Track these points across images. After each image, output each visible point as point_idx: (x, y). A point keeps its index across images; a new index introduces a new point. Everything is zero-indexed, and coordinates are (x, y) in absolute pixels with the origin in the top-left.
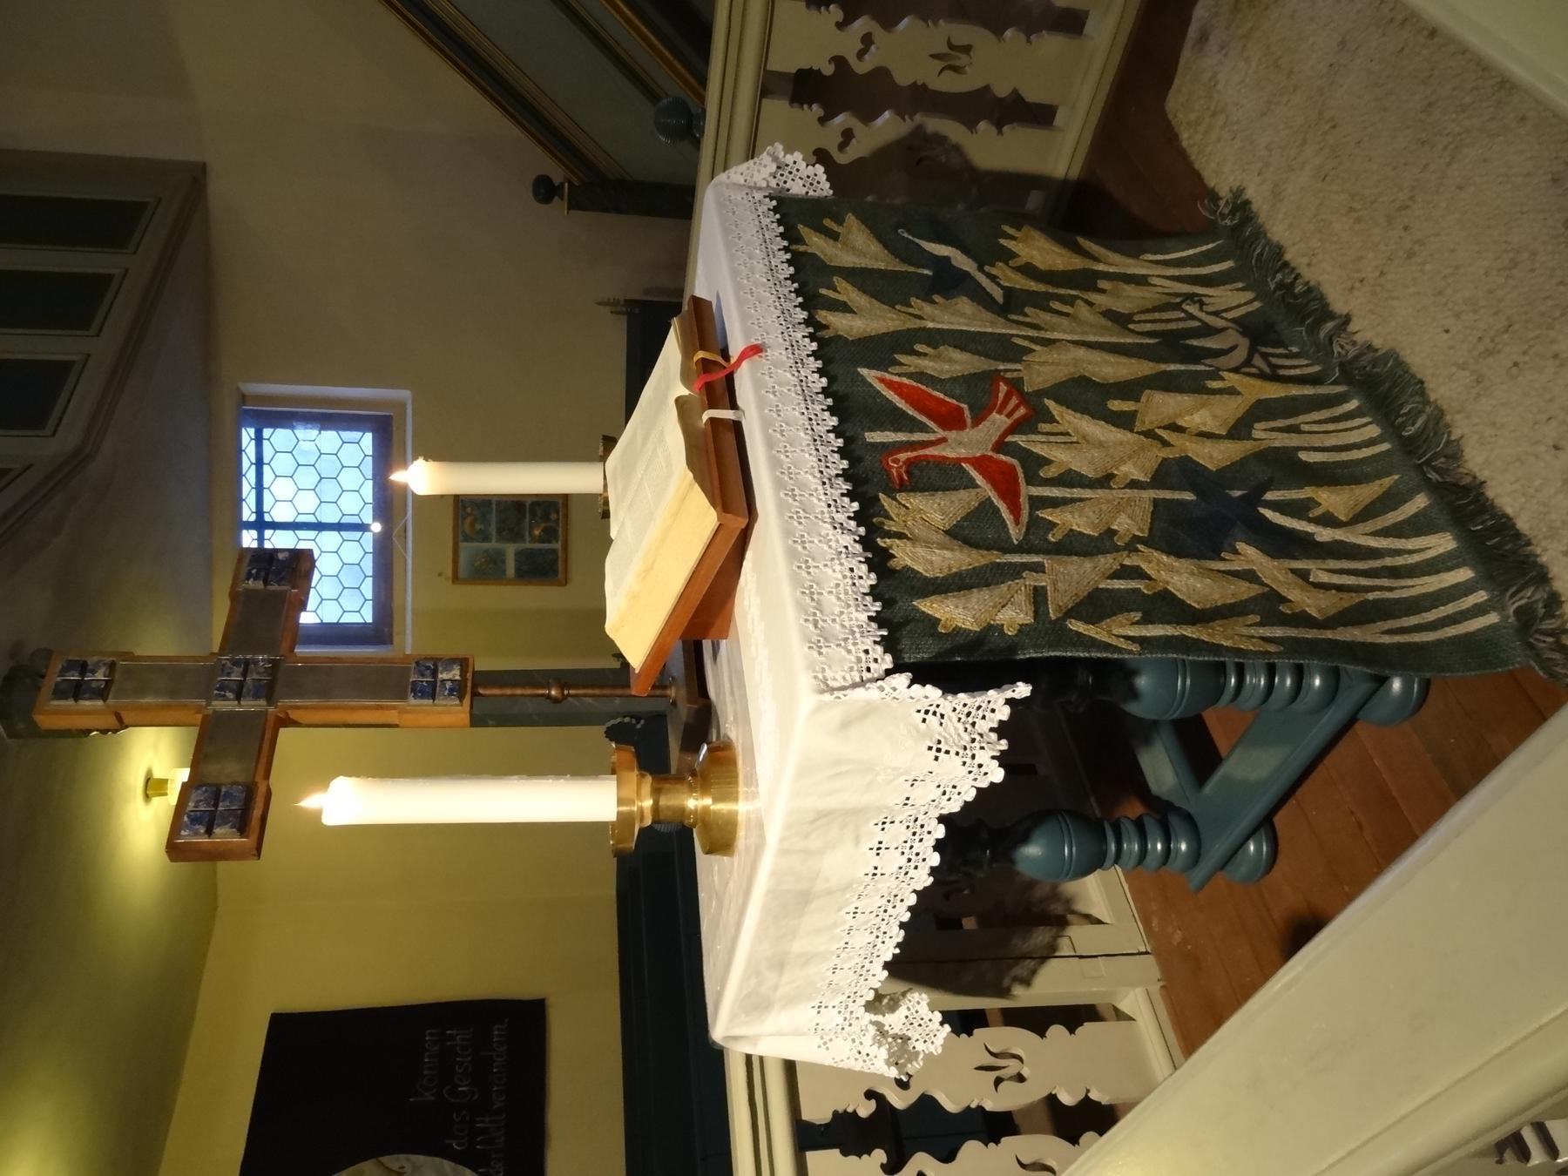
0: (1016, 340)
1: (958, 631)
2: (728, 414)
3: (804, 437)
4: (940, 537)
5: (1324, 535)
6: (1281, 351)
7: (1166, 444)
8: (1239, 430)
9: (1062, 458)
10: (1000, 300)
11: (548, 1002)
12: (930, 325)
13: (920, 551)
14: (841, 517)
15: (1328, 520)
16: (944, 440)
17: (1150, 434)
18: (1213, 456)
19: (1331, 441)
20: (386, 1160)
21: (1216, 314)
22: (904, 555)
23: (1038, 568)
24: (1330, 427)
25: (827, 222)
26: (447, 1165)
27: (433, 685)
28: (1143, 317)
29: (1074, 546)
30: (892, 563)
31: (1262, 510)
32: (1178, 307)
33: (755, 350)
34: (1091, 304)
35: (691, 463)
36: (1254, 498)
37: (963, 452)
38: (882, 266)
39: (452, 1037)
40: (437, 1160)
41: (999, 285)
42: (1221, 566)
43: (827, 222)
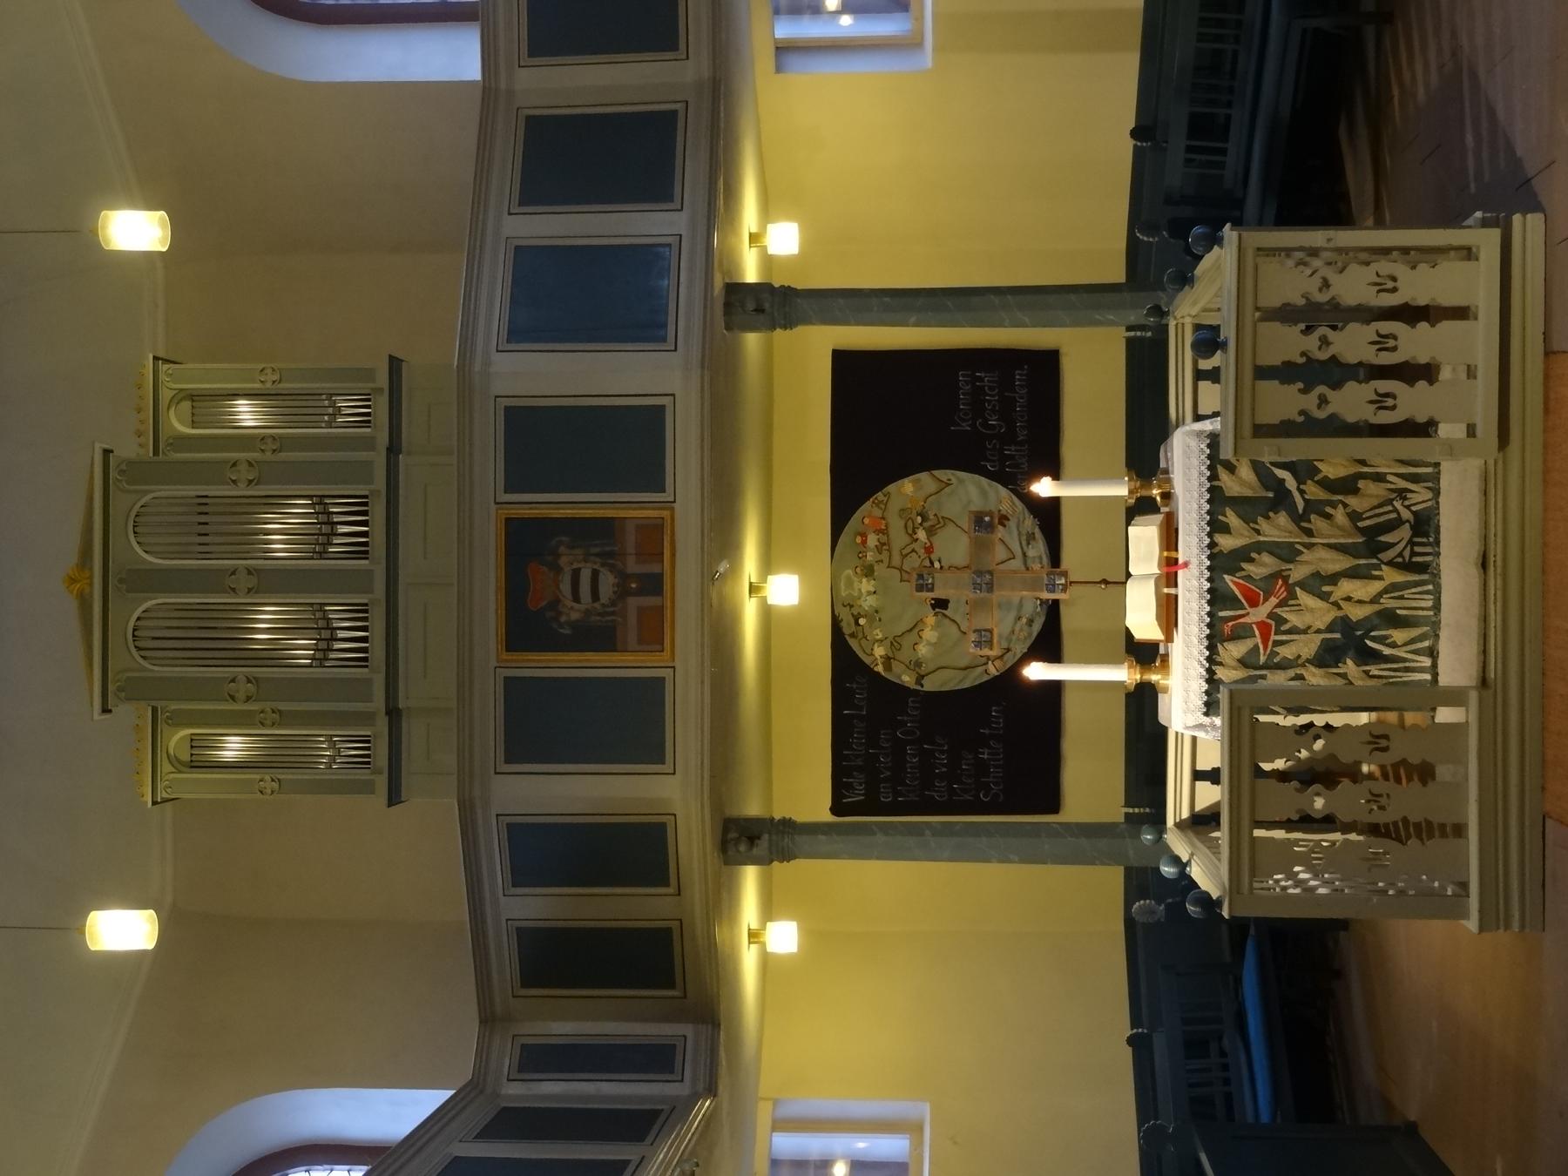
2: (1172, 591)
4: (1235, 664)
5: (1387, 651)
7: (1340, 608)
8: (1374, 600)
9: (1294, 619)
15: (1394, 645)
17: (1336, 605)
18: (1356, 613)
19: (1414, 604)
20: (936, 473)
21: (1408, 507)
22: (1221, 673)
23: (1263, 677)
26: (984, 481)
29: (1283, 666)
33: (1186, 565)
34: (1345, 505)
35: (1158, 618)
36: (1366, 635)
38: (1249, 493)
39: (981, 379)
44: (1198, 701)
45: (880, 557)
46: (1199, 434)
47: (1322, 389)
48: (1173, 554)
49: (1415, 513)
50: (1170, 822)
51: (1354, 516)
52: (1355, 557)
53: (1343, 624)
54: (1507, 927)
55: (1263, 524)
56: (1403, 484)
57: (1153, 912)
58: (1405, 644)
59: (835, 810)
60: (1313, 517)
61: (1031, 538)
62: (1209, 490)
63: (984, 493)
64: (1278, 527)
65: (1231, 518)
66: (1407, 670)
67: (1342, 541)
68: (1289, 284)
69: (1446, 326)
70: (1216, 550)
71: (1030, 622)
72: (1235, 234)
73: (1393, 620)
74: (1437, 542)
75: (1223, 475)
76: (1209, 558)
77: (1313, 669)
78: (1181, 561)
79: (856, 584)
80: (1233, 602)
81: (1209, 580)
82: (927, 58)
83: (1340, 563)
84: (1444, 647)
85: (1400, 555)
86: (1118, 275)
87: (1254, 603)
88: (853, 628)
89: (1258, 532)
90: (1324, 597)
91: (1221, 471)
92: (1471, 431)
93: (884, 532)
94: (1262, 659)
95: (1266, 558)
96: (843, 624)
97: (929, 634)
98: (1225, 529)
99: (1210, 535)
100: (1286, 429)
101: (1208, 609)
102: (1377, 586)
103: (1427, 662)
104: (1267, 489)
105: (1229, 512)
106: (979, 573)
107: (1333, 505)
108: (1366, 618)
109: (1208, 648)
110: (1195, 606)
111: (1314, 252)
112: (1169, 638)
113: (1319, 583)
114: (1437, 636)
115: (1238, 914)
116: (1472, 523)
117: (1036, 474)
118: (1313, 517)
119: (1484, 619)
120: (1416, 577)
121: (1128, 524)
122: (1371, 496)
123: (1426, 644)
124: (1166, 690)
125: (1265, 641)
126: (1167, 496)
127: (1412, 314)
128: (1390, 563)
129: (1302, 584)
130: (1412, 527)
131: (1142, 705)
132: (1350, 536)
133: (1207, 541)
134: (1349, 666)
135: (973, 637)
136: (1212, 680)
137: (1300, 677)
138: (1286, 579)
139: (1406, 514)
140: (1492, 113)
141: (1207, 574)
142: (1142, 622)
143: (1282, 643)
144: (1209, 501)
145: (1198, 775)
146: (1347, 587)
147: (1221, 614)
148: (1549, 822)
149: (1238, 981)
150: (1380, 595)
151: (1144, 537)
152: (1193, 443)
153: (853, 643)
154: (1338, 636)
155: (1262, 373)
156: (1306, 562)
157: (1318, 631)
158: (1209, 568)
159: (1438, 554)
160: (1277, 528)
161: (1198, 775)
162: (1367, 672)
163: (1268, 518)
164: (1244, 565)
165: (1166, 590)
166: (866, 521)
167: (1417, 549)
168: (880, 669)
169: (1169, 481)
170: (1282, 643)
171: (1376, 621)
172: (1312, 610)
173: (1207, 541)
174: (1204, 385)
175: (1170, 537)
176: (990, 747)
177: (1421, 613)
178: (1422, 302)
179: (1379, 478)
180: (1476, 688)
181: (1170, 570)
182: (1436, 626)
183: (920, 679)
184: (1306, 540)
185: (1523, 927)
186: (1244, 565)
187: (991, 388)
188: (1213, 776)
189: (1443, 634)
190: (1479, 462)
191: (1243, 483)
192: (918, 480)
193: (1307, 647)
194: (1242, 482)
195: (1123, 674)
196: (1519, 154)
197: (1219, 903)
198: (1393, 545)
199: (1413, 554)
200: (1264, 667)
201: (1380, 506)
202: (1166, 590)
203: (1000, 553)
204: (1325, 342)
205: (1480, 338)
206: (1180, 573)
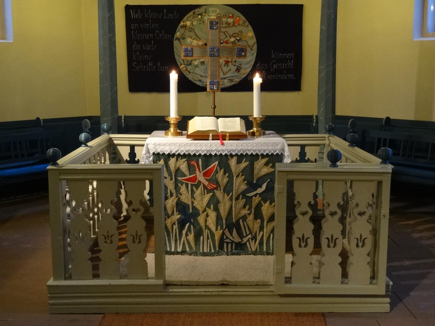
0: (231, 194)
2: (211, 138)
3: (198, 149)
4: (177, 166)
5: (184, 232)
6: (234, 248)
7: (203, 212)
8: (207, 227)
9: (198, 192)
10: (247, 195)
11: (300, 92)
12: (235, 178)
13: (174, 162)
14: (179, 151)
15: (187, 235)
16: (200, 172)
17: (205, 211)
18: (201, 219)
19: (205, 244)
21: (248, 241)
23: (171, 179)
24: (209, 245)
25: (271, 165)
27: (213, 84)
28: (245, 224)
29: (177, 188)
30: (171, 158)
31: (188, 224)
32: (251, 233)
33: (223, 144)
34: (249, 214)
35: (198, 131)
36: (191, 223)
37: (198, 175)
38: (255, 172)
39: (290, 62)
40: (254, 60)
41: (252, 196)
42: (175, 210)
43: (271, 165)
44: (160, 150)
45: (224, 23)
46: (283, 150)
47: (310, 213)
48: (227, 138)
49: (246, 243)
50: (112, 136)
51: (244, 218)
52: (226, 219)
53: (196, 213)
54: (51, 298)
55: (241, 178)
56: (259, 239)
58: (187, 240)
59: (128, 8)
61: (231, 81)
63: (248, 63)
64: (240, 185)
65: (244, 164)
66: (176, 241)
67: (234, 213)
69: (339, 269)
70: (229, 157)
71: (200, 81)
72: (391, 171)
73: (198, 234)
74: (233, 254)
75: (264, 160)
76: (226, 155)
77: (175, 201)
78: (224, 142)
79: (214, 14)
80: (205, 165)
81: (216, 154)
82: (418, 39)
83: (224, 212)
84: (186, 258)
85: (227, 238)
86: (339, 112)
87: (205, 175)
88: (197, 13)
89: (238, 176)
90: (208, 205)
91: (266, 160)
92: (288, 280)
93: (234, 25)
94: (180, 178)
95: (226, 180)
96: (198, 9)
97: (195, 43)
98: (239, 162)
99: (236, 155)
102: (213, 228)
103: (179, 250)
104: (257, 180)
105: (247, 163)
106: (218, 50)
107: (250, 209)
108: (199, 224)
109: (184, 154)
110: (204, 148)
112: (189, 136)
113: (214, 203)
114: (190, 254)
115: (49, 174)
116: (242, 277)
119: (198, 285)
120: (217, 245)
121: (242, 117)
122: (254, 225)
123: (188, 249)
124: (166, 134)
125: (188, 180)
126: (253, 134)
128: (223, 234)
129: (214, 195)
130: (239, 242)
131: (158, 124)
132: (236, 216)
133: (234, 154)
135: (189, 48)
136: (170, 156)
137: (172, 195)
138: (216, 188)
139: (245, 240)
140: (423, 276)
141: (218, 154)
142: (197, 124)
143: (187, 187)
144: (252, 154)
145: (132, 147)
146: (213, 215)
147: (200, 160)
150: (209, 229)
151: (235, 125)
152: (279, 147)
153: (191, 13)
154: (191, 211)
157: (193, 203)
158: (221, 154)
159: (228, 255)
160: (239, 184)
162: (174, 224)
163: (244, 180)
164: (222, 170)
165: (211, 135)
166: (238, 18)
167: (230, 245)
168: (182, 24)
169: (260, 135)
170: (187, 187)
171: (197, 228)
172: (202, 200)
173: (234, 154)
174: (298, 149)
175: (235, 136)
176: (153, 66)
177: (201, 246)
179: (261, 228)
180: (165, 281)
181: (220, 137)
182: (195, 254)
183: (178, 39)
184: (234, 197)
185: (51, 304)
186: (222, 170)
187: (287, 66)
188: (132, 154)
189: (192, 258)
191: (260, 170)
192: (253, 38)
193: (186, 198)
194: (261, 169)
195: (173, 115)
196: (412, 293)
197: (55, 164)
199: (228, 243)
200: (176, 180)
202: (211, 135)
203: (225, 69)
205: (331, 283)
206: (219, 142)
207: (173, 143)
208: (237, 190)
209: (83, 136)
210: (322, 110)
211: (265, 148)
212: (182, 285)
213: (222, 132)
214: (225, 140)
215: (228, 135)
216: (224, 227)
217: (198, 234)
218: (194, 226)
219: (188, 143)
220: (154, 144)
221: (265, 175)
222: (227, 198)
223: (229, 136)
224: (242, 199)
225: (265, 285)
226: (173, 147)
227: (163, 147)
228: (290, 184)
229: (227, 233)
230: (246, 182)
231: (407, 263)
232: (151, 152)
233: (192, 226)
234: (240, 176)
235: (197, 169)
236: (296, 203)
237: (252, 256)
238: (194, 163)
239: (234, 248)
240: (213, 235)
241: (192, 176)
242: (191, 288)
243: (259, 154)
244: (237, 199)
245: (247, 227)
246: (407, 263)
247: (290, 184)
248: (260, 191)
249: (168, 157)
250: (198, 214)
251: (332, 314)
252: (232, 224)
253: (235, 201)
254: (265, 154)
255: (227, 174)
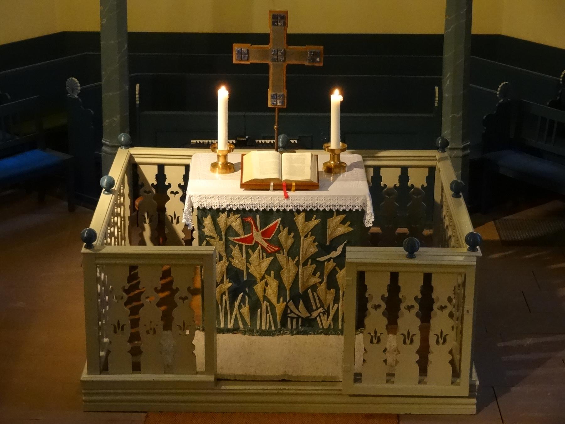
0: (297, 258)
1: (203, 221)
2: (271, 188)
4: (229, 223)
5: (236, 304)
6: (300, 324)
7: (261, 280)
8: (266, 298)
9: (254, 256)
10: (318, 259)
12: (302, 239)
13: (224, 219)
15: (240, 307)
16: (258, 231)
17: (264, 278)
18: (258, 289)
19: (263, 319)
21: (319, 315)
23: (221, 239)
24: (268, 321)
25: (349, 223)
29: (228, 250)
30: (220, 213)
31: (242, 294)
33: (287, 197)
34: (321, 283)
36: (245, 293)
37: (254, 234)
38: (329, 232)
43: (349, 223)
44: (206, 204)
46: (365, 205)
47: (384, 306)
48: (293, 188)
49: (316, 318)
51: (314, 287)
52: (291, 289)
53: (252, 281)
55: (310, 239)
57: (73, 90)
58: (241, 314)
60: (314, 265)
62: (331, 210)
64: (309, 247)
65: (314, 222)
66: (226, 314)
67: (300, 281)
68: (442, 291)
69: (417, 368)
70: (295, 214)
73: (255, 306)
74: (299, 333)
76: (291, 210)
77: (226, 266)
78: (290, 193)
80: (264, 223)
81: (278, 210)
83: (287, 283)
87: (264, 234)
89: (306, 236)
90: (268, 272)
92: (358, 378)
94: (231, 239)
95: (290, 242)
99: (304, 210)
100: (362, 287)
101: (261, 210)
102: (274, 300)
103: (231, 326)
104: (331, 241)
105: (318, 221)
107: (321, 276)
109: (238, 209)
111: (460, 306)
113: (275, 269)
114: (244, 333)
117: (344, 94)
118: (314, 265)
119: (254, 380)
122: (326, 296)
123: (241, 326)
125: (242, 240)
127: (424, 353)
128: (287, 307)
129: (275, 259)
130: (307, 318)
132: (303, 285)
133: (301, 209)
134: (227, 285)
136: (219, 211)
137: (221, 258)
138: (278, 252)
139: (315, 314)
140: (539, 363)
144: (324, 210)
145: (161, 167)
146: (273, 284)
147: (258, 217)
148: (144, 415)
149: (32, 145)
150: (269, 301)
152: (359, 202)
154: (245, 278)
155: (394, 277)
156: (287, 262)
157: (248, 268)
158: (285, 210)
160: (308, 246)
161: (161, 167)
162: (224, 293)
163: (314, 242)
164: (286, 229)
165: (272, 184)
167: (295, 321)
172: (260, 265)
174: (398, 171)
177: (258, 322)
178: (430, 357)
179: (336, 300)
180: (216, 375)
182: (251, 332)
184: (301, 263)
185: (85, 401)
186: (286, 229)
190: (341, 377)
191: (335, 229)
193: (239, 262)
196: (513, 389)
198: (297, 307)
199: (292, 318)
200: (227, 241)
201: (320, 301)
202: (272, 184)
204: (410, 308)
207: (223, 196)
208: (306, 253)
209: (106, 180)
210: (448, 83)
211: (341, 203)
212: (236, 380)
213: (286, 180)
214: (290, 190)
215: (294, 184)
216: (288, 299)
217: (255, 306)
218: (249, 297)
219: (242, 196)
220: (199, 196)
221: (341, 235)
222: (292, 263)
223: (296, 185)
224: (311, 264)
225: (332, 381)
226: (223, 201)
227: (210, 200)
228: (361, 276)
229: (292, 306)
230: (316, 243)
231: (529, 341)
232: (195, 207)
233: (246, 297)
234: (309, 236)
235: (254, 227)
236: (367, 295)
237: (323, 336)
238: (249, 219)
239: (300, 324)
240: (273, 308)
241: (247, 236)
242: (245, 385)
243: (334, 210)
244: (305, 264)
245: (317, 299)
246: (529, 341)
247: (361, 276)
248: (334, 254)
249: (215, 213)
250: (255, 283)
251: (409, 416)
252: (298, 295)
253: (303, 266)
254: (341, 210)
255: (292, 234)
